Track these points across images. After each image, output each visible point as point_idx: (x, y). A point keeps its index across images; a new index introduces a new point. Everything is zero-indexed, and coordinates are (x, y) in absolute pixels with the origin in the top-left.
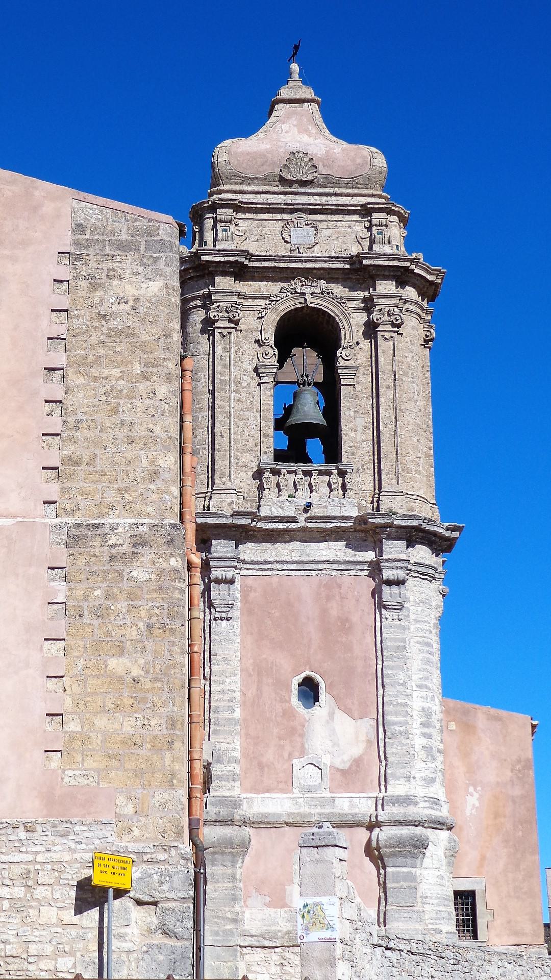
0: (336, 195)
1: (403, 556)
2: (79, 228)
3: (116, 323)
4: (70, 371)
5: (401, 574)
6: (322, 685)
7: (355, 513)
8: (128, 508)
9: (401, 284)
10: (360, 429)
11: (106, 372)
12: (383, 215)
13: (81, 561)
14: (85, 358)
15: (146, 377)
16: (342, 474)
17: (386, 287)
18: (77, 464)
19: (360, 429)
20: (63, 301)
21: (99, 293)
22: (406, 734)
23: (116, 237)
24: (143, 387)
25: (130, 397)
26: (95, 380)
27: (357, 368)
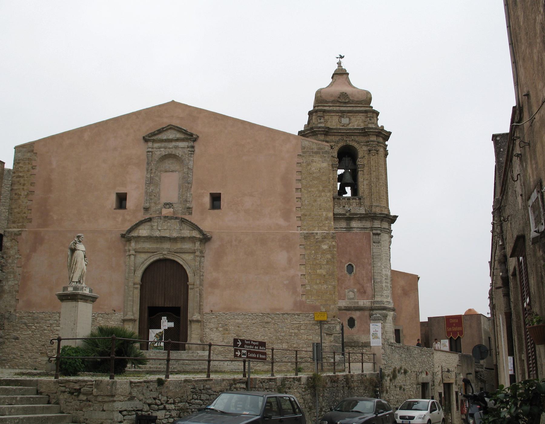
0: (356, 107)
1: (379, 226)
2: (303, 148)
3: (314, 175)
4: (303, 189)
5: (379, 232)
6: (354, 267)
7: (364, 212)
8: (320, 228)
9: (377, 136)
10: (365, 185)
11: (313, 190)
12: (371, 114)
13: (308, 243)
14: (306, 185)
15: (324, 191)
16: (360, 199)
17: (373, 138)
18: (306, 216)
19: (365, 185)
20: (300, 169)
21: (310, 167)
22: (381, 282)
23: (314, 150)
24: (323, 194)
25: (319, 197)
26: (310, 192)
27: (364, 165)
